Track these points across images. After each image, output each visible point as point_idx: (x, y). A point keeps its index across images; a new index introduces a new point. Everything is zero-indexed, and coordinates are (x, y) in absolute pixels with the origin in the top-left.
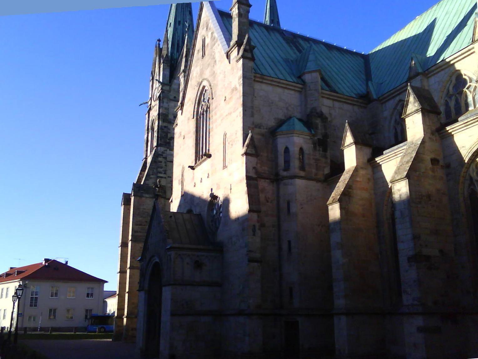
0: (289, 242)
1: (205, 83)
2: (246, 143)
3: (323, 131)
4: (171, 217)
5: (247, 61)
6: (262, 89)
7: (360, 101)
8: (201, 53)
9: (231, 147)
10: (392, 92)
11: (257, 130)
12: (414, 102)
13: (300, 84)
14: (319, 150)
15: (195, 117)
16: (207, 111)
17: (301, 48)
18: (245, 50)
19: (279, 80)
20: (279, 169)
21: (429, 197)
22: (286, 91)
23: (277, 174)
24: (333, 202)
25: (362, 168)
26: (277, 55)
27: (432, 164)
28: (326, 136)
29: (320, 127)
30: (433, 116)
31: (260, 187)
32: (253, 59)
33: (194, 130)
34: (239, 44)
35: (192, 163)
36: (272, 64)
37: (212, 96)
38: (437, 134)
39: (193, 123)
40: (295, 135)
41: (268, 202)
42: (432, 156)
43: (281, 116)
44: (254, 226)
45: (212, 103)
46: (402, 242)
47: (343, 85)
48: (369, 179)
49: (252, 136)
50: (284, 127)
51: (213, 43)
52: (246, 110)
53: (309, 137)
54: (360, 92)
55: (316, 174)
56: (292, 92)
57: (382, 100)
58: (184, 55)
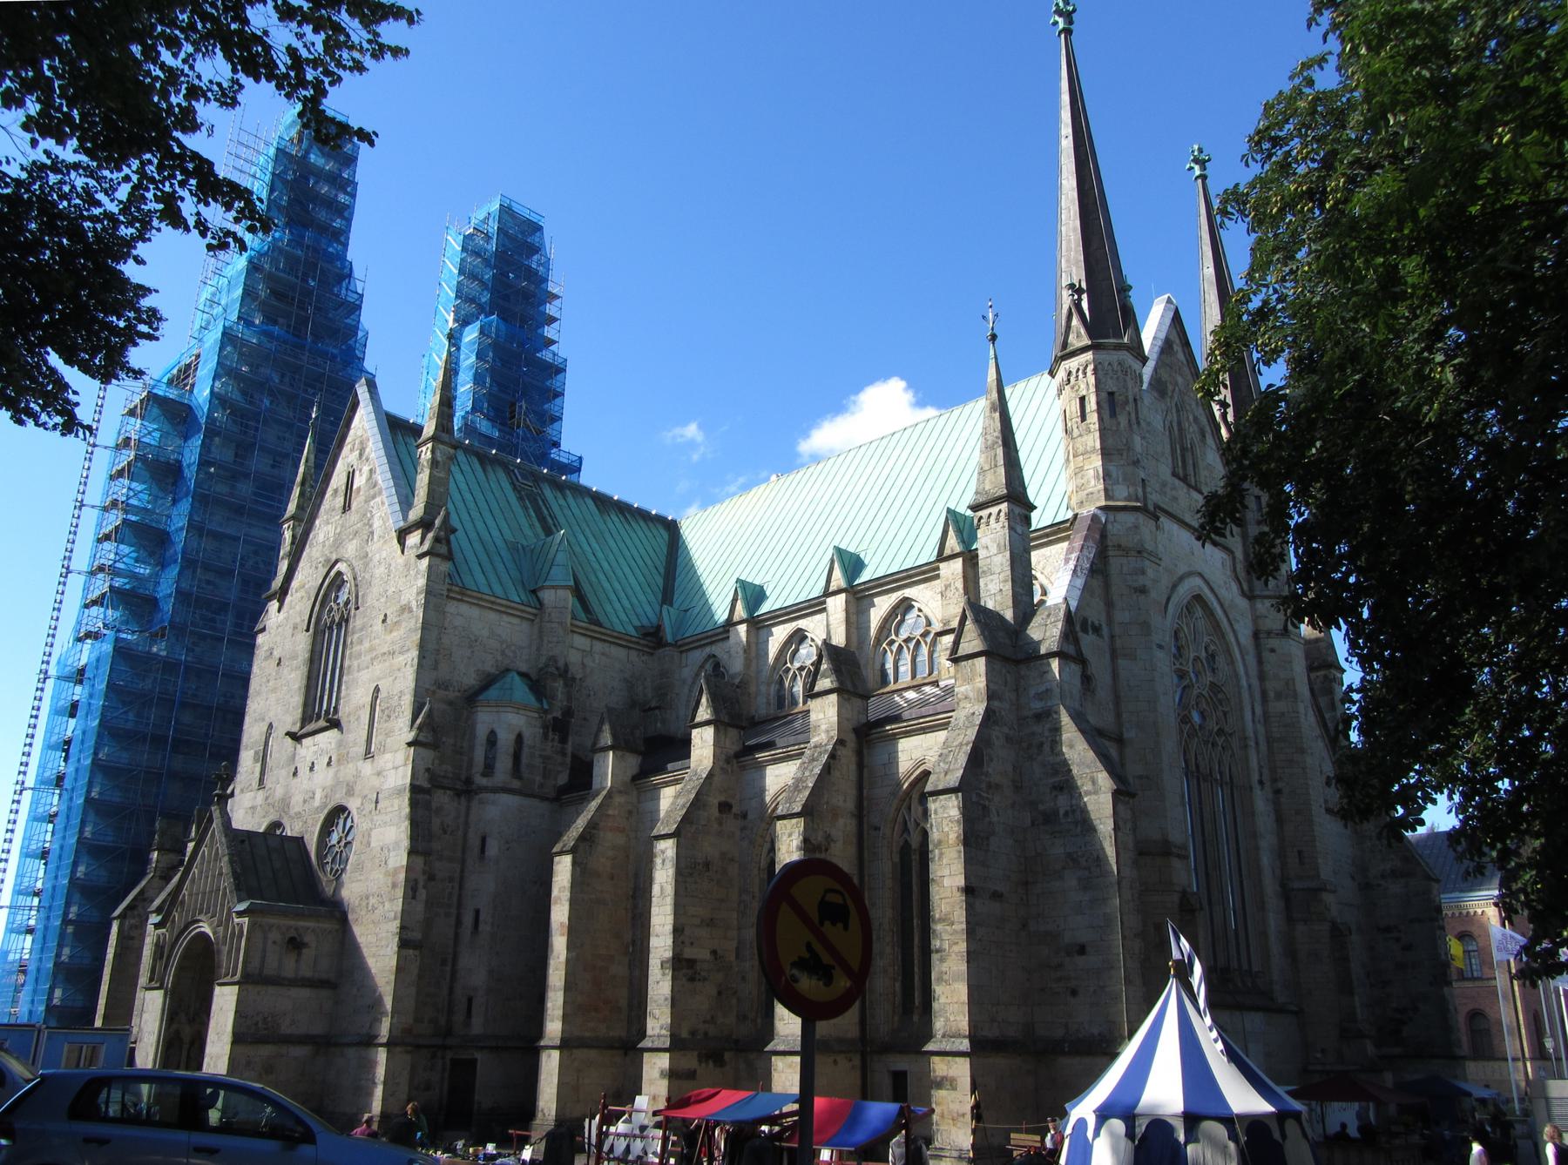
0: (477, 912)
1: (341, 567)
2: (419, 721)
3: (565, 703)
4: (243, 841)
5: (437, 560)
6: (463, 614)
7: (642, 642)
8: (340, 500)
9: (386, 721)
10: (699, 637)
11: (441, 693)
12: (707, 707)
13: (531, 607)
14: (553, 740)
15: (311, 630)
16: (339, 626)
17: (546, 512)
18: (437, 540)
19: (493, 599)
20: (473, 771)
21: (707, 865)
22: (505, 617)
23: (469, 781)
24: (561, 853)
25: (620, 792)
26: (495, 533)
27: (720, 811)
28: (568, 712)
29: (560, 696)
30: (733, 733)
31: (434, 805)
32: (449, 557)
33: (307, 655)
34: (425, 524)
35: (294, 724)
36: (484, 558)
37: (357, 603)
38: (735, 761)
39: (303, 642)
40: (509, 709)
41: (445, 832)
42: (723, 799)
43: (489, 667)
44: (416, 881)
45: (355, 616)
46: (657, 936)
47: (617, 605)
48: (630, 812)
49: (430, 710)
50: (492, 693)
51: (372, 492)
52: (424, 657)
53: (536, 715)
54: (645, 622)
55: (542, 786)
56: (515, 621)
57: (680, 646)
58: (299, 478)
